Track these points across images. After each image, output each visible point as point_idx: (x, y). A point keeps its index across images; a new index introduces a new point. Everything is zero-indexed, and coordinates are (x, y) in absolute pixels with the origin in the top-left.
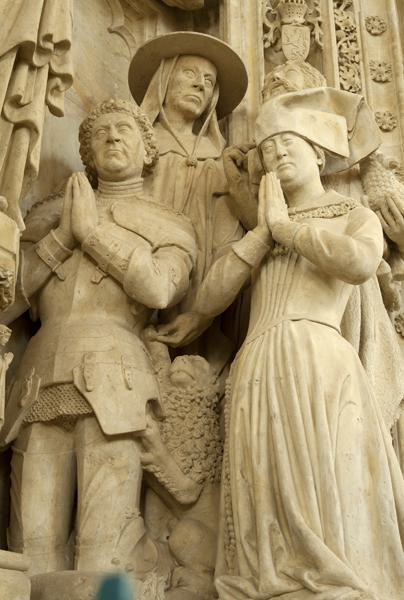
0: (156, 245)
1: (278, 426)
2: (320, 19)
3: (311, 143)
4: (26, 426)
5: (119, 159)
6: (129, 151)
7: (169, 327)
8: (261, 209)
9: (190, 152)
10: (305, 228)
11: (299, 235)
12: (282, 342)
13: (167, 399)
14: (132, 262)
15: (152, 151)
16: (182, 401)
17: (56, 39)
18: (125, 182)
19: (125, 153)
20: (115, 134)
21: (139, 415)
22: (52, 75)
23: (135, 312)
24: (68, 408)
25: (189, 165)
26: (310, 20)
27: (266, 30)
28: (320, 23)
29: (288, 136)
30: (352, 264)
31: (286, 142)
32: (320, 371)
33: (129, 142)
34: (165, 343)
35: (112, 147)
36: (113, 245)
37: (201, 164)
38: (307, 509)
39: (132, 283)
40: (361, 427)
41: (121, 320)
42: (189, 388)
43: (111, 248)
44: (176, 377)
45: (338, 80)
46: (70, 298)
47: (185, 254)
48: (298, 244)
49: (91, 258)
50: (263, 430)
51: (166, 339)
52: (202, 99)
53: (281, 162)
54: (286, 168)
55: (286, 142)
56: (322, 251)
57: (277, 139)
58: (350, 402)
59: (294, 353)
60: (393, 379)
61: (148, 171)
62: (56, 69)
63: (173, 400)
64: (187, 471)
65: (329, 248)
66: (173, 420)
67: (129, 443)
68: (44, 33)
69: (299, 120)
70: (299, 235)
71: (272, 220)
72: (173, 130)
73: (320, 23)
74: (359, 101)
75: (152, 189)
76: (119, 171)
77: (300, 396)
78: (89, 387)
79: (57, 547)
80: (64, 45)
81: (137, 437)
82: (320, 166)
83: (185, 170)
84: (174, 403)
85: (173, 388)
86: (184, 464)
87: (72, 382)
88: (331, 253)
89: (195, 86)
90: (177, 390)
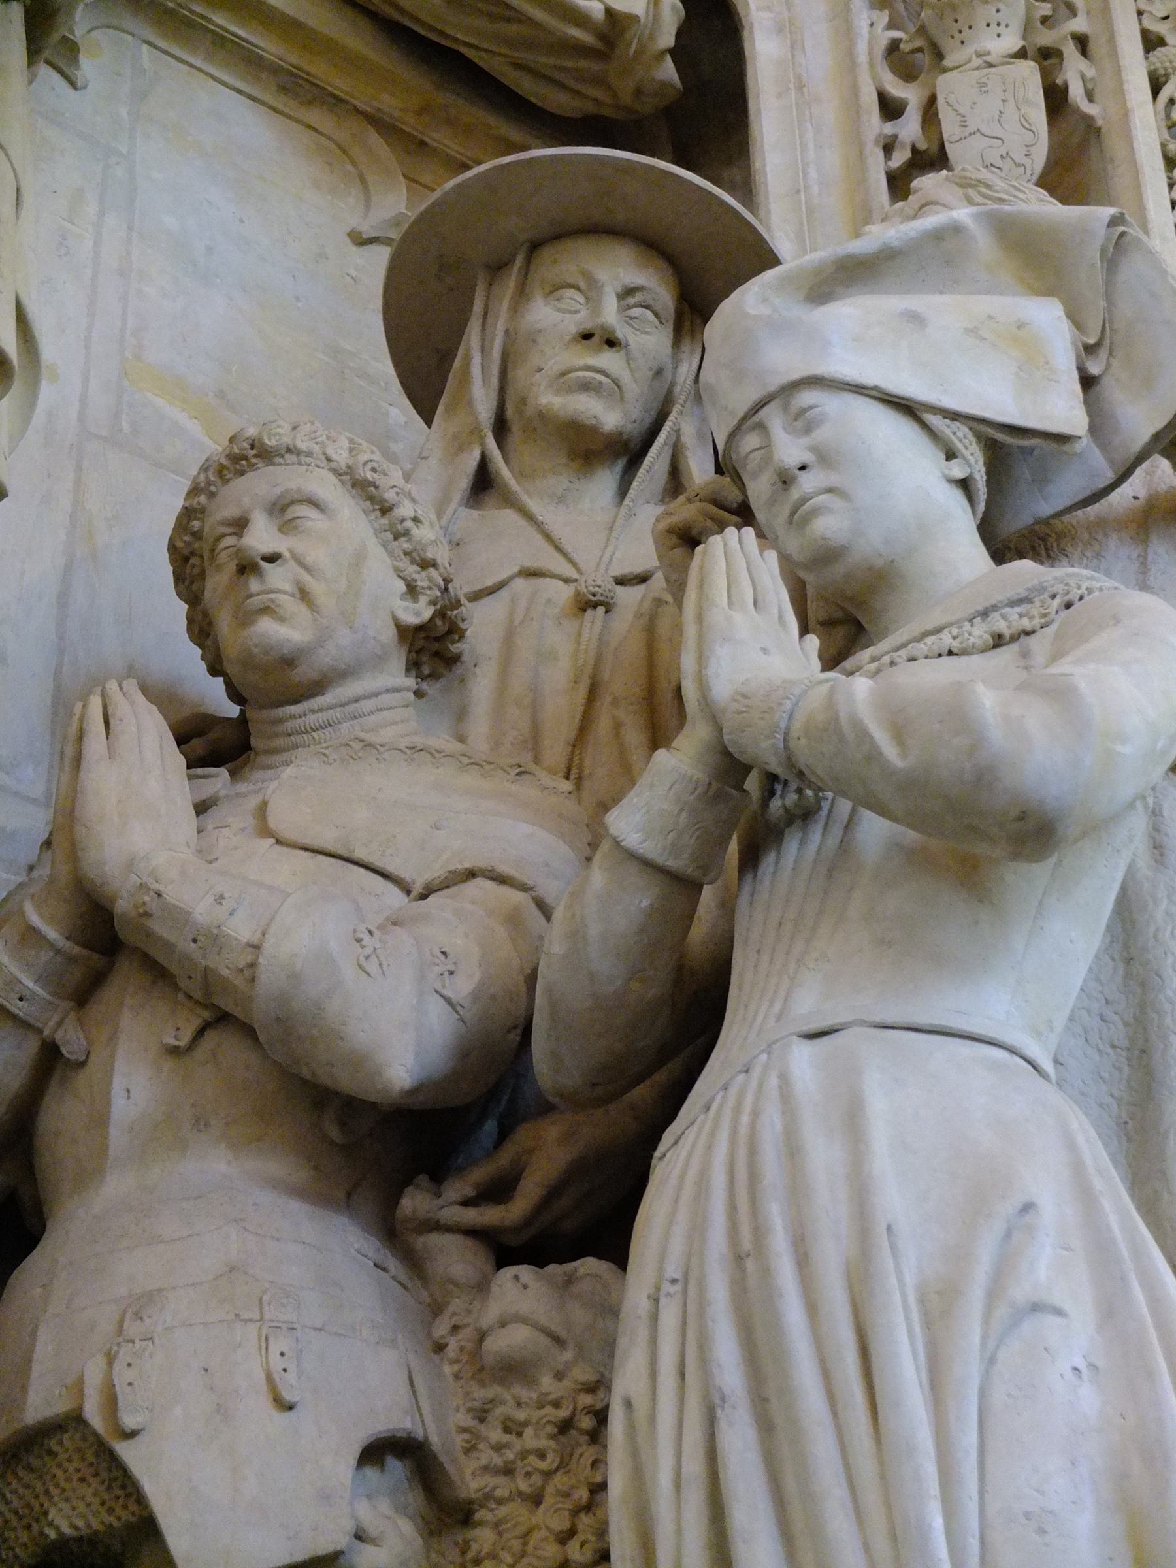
1: (739, 1441)
2: (1079, 24)
3: (907, 408)
5: (281, 619)
6: (316, 588)
8: (688, 662)
9: (587, 560)
11: (797, 726)
12: (756, 1114)
13: (477, 1436)
14: (267, 948)
15: (422, 579)
16: (529, 1432)
20: (261, 537)
21: (325, 1497)
23: (334, 1133)
25: (586, 604)
26: (1046, 38)
27: (890, 109)
28: (1082, 43)
29: (807, 397)
30: (984, 777)
31: (804, 423)
32: (894, 1201)
33: (316, 554)
34: (472, 1232)
35: (254, 585)
36: (210, 899)
37: (628, 597)
39: (285, 1023)
40: (1089, 1400)
41: (279, 1166)
42: (547, 1382)
44: (500, 1343)
47: (517, 897)
48: (804, 754)
49: (159, 973)
50: (694, 1466)
52: (626, 377)
53: (795, 494)
55: (804, 423)
56: (874, 755)
58: (1036, 1308)
59: (793, 1150)
61: (432, 649)
63: (496, 1435)
65: (899, 735)
66: (502, 1511)
69: (857, 339)
70: (797, 726)
71: (722, 687)
72: (534, 505)
73: (1082, 43)
74: (1101, 232)
75: (461, 714)
76: (289, 662)
77: (812, 1308)
78: (129, 1421)
82: (964, 484)
83: (571, 625)
84: (498, 1448)
85: (494, 1391)
88: (904, 754)
89: (587, 336)
90: (511, 1400)
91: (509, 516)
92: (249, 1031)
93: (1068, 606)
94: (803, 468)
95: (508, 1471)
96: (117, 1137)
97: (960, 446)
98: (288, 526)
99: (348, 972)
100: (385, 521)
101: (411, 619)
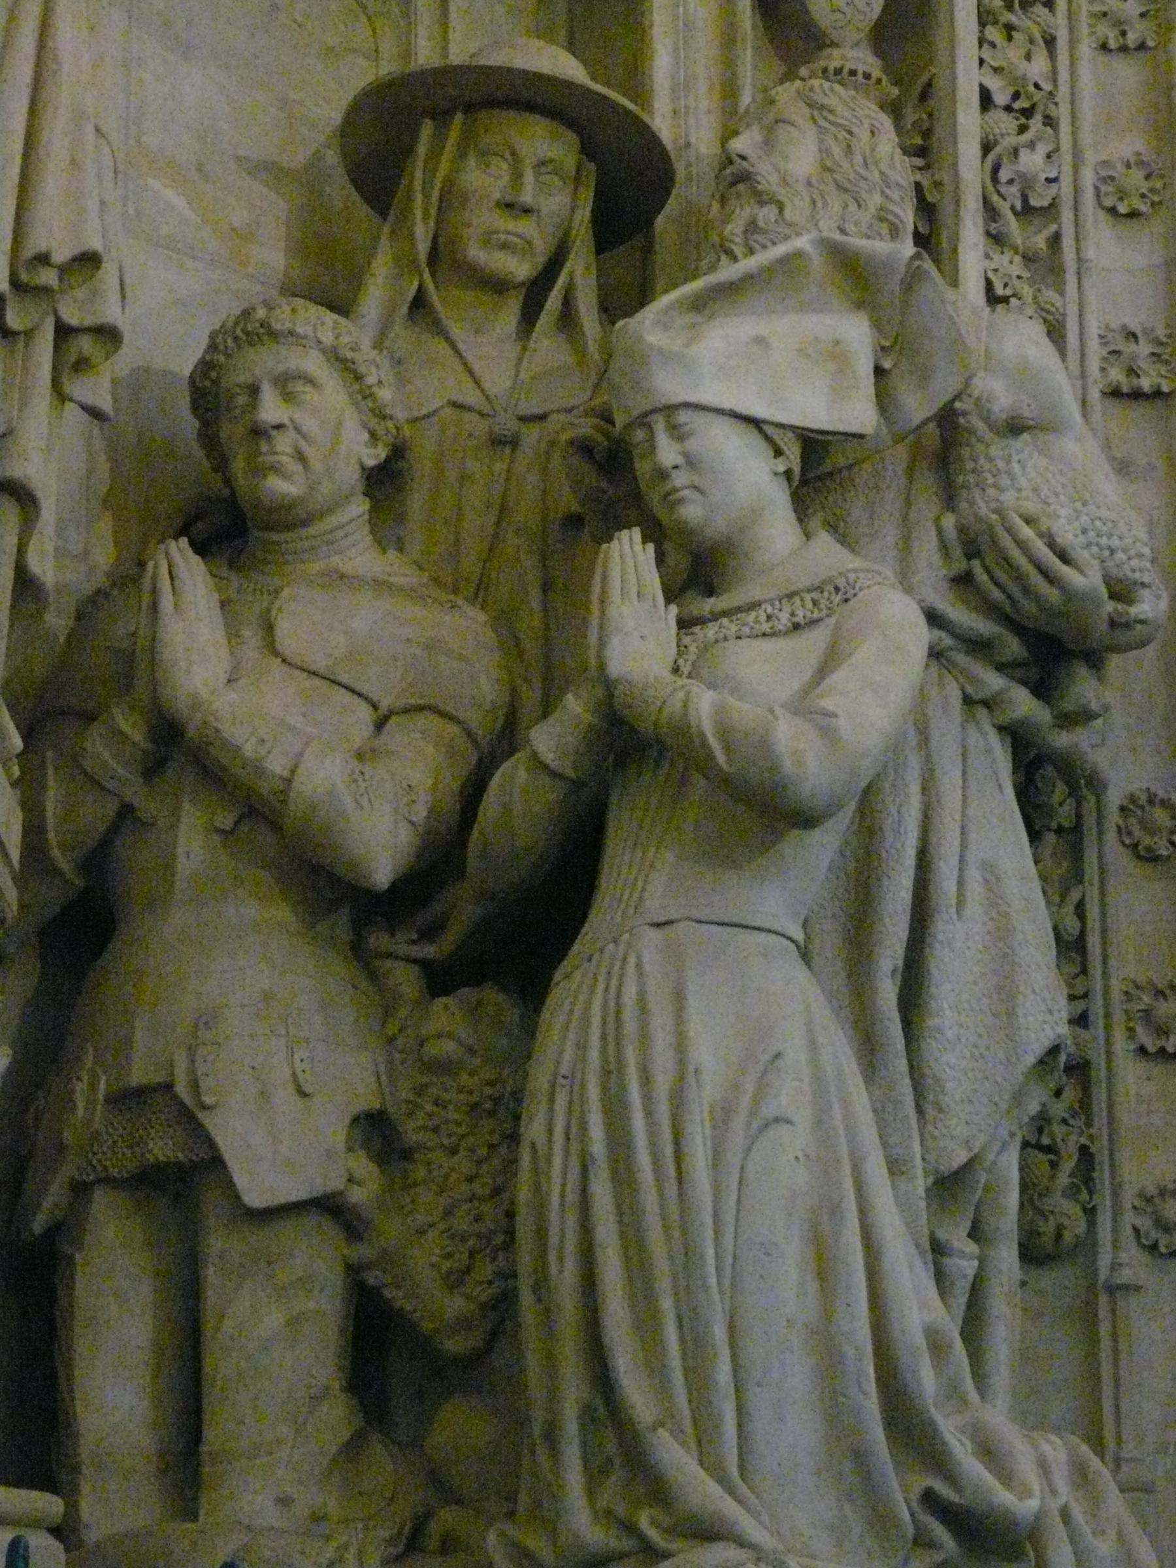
0: (385, 704)
4: (80, 1190)
6: (309, 452)
7: (423, 918)
10: (681, 695)
17: (60, 256)
18: (311, 531)
19: (301, 457)
20: (271, 409)
21: (329, 1154)
22: (63, 332)
24: (162, 1148)
29: (683, 417)
31: (678, 433)
33: (311, 425)
36: (253, 740)
37: (532, 435)
38: (655, 1368)
43: (249, 750)
45: (968, 78)
46: (168, 866)
47: (453, 729)
51: (416, 951)
54: (681, 501)
55: (678, 433)
57: (659, 424)
58: (777, 1120)
60: (1011, 1013)
61: (385, 481)
62: (72, 317)
63: (429, 1107)
64: (455, 1280)
65: (728, 749)
67: (311, 1221)
68: (28, 252)
71: (615, 669)
72: (457, 331)
75: (401, 519)
77: (649, 1113)
78: (208, 1100)
79: (163, 1471)
80: (89, 261)
81: (330, 1207)
82: (788, 474)
84: (430, 1115)
86: (446, 1265)
87: (169, 1087)
88: (729, 761)
91: (440, 347)
92: (276, 827)
93: (846, 600)
94: (676, 467)
95: (436, 1130)
96: (180, 885)
97: (785, 448)
98: (288, 397)
99: (348, 800)
100: (356, 387)
101: (371, 463)
